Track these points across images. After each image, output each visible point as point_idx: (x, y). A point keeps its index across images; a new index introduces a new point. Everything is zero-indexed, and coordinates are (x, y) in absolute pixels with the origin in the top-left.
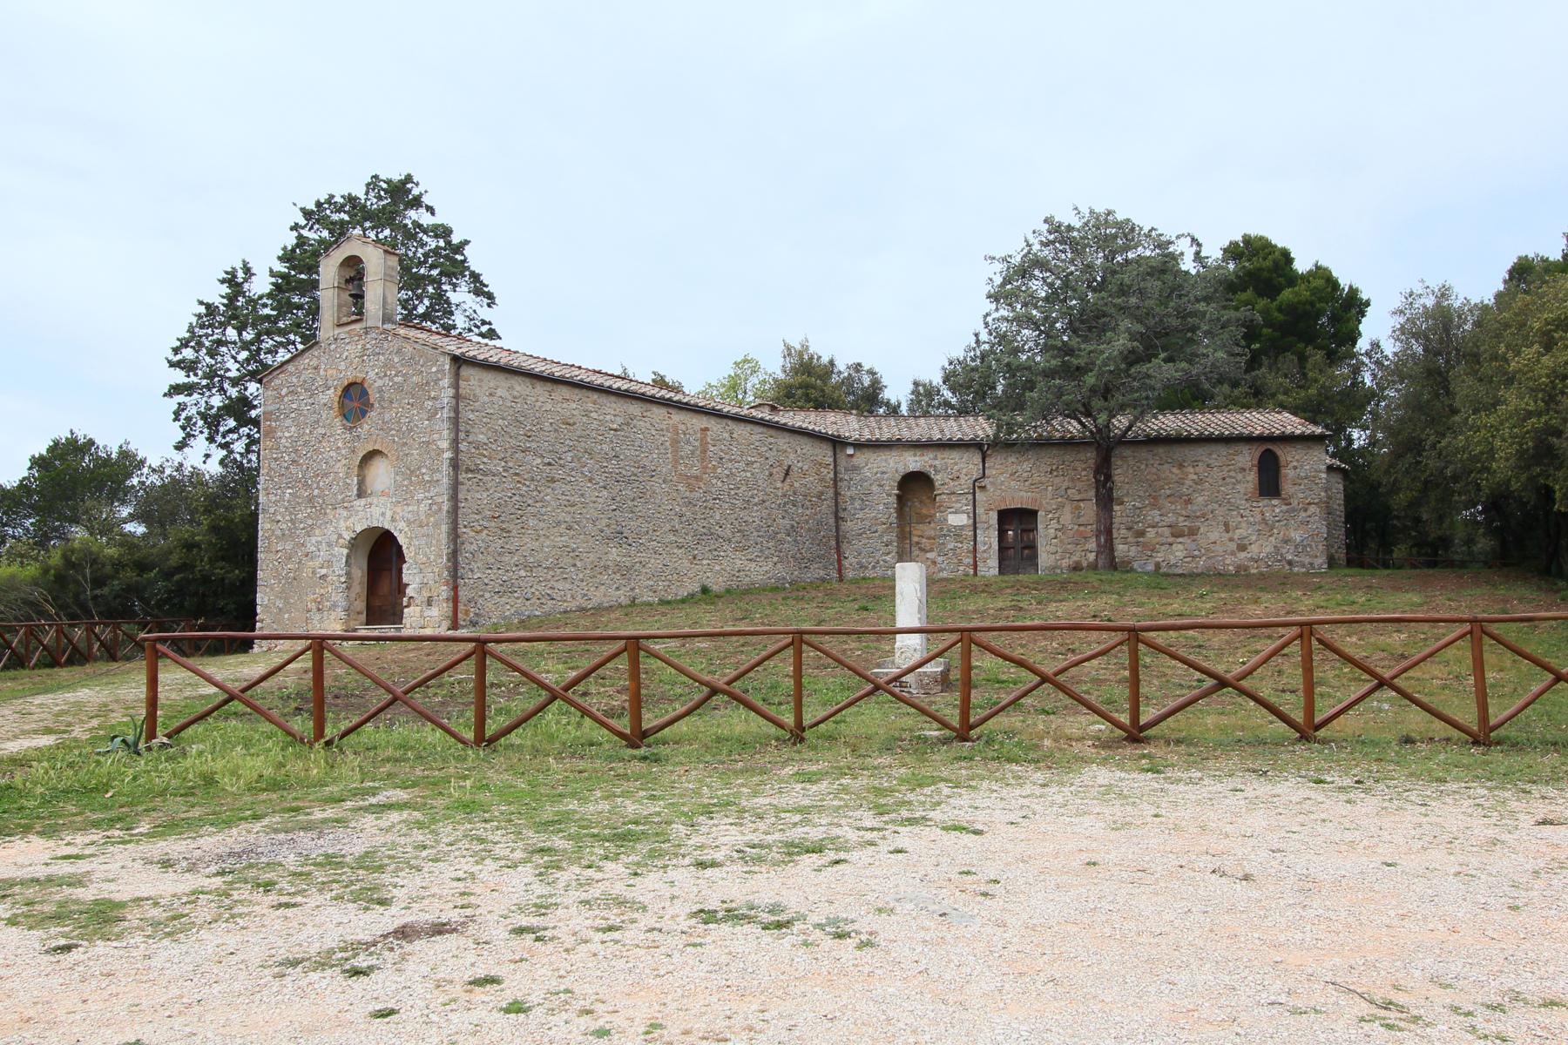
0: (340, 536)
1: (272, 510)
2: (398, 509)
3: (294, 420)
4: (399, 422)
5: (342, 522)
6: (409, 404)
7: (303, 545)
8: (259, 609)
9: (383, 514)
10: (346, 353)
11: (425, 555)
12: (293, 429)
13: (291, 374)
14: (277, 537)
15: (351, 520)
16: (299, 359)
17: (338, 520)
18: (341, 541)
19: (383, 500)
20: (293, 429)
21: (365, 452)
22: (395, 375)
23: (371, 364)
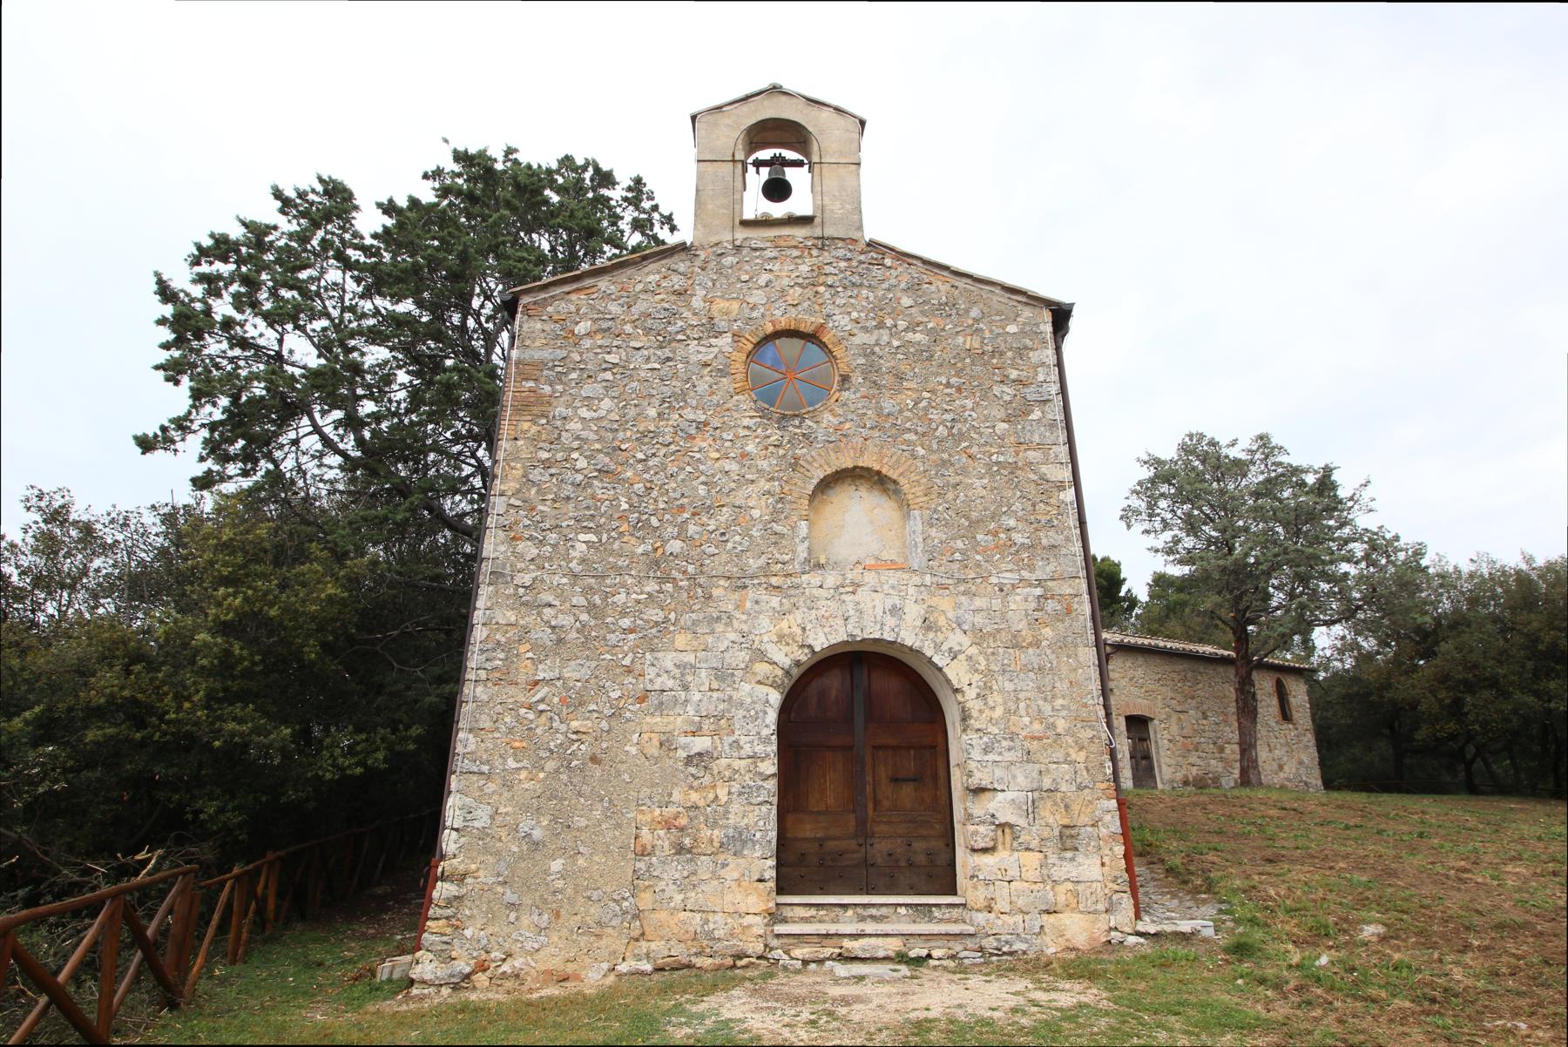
0: (760, 655)
1: (527, 579)
2: (944, 603)
5: (764, 622)
6: (948, 385)
8: (449, 842)
9: (895, 611)
10: (764, 278)
11: (1039, 716)
12: (607, 404)
13: (607, 296)
15: (798, 616)
16: (630, 271)
17: (752, 616)
18: (762, 669)
19: (893, 578)
20: (607, 404)
21: (829, 471)
22: (906, 330)
23: (839, 301)
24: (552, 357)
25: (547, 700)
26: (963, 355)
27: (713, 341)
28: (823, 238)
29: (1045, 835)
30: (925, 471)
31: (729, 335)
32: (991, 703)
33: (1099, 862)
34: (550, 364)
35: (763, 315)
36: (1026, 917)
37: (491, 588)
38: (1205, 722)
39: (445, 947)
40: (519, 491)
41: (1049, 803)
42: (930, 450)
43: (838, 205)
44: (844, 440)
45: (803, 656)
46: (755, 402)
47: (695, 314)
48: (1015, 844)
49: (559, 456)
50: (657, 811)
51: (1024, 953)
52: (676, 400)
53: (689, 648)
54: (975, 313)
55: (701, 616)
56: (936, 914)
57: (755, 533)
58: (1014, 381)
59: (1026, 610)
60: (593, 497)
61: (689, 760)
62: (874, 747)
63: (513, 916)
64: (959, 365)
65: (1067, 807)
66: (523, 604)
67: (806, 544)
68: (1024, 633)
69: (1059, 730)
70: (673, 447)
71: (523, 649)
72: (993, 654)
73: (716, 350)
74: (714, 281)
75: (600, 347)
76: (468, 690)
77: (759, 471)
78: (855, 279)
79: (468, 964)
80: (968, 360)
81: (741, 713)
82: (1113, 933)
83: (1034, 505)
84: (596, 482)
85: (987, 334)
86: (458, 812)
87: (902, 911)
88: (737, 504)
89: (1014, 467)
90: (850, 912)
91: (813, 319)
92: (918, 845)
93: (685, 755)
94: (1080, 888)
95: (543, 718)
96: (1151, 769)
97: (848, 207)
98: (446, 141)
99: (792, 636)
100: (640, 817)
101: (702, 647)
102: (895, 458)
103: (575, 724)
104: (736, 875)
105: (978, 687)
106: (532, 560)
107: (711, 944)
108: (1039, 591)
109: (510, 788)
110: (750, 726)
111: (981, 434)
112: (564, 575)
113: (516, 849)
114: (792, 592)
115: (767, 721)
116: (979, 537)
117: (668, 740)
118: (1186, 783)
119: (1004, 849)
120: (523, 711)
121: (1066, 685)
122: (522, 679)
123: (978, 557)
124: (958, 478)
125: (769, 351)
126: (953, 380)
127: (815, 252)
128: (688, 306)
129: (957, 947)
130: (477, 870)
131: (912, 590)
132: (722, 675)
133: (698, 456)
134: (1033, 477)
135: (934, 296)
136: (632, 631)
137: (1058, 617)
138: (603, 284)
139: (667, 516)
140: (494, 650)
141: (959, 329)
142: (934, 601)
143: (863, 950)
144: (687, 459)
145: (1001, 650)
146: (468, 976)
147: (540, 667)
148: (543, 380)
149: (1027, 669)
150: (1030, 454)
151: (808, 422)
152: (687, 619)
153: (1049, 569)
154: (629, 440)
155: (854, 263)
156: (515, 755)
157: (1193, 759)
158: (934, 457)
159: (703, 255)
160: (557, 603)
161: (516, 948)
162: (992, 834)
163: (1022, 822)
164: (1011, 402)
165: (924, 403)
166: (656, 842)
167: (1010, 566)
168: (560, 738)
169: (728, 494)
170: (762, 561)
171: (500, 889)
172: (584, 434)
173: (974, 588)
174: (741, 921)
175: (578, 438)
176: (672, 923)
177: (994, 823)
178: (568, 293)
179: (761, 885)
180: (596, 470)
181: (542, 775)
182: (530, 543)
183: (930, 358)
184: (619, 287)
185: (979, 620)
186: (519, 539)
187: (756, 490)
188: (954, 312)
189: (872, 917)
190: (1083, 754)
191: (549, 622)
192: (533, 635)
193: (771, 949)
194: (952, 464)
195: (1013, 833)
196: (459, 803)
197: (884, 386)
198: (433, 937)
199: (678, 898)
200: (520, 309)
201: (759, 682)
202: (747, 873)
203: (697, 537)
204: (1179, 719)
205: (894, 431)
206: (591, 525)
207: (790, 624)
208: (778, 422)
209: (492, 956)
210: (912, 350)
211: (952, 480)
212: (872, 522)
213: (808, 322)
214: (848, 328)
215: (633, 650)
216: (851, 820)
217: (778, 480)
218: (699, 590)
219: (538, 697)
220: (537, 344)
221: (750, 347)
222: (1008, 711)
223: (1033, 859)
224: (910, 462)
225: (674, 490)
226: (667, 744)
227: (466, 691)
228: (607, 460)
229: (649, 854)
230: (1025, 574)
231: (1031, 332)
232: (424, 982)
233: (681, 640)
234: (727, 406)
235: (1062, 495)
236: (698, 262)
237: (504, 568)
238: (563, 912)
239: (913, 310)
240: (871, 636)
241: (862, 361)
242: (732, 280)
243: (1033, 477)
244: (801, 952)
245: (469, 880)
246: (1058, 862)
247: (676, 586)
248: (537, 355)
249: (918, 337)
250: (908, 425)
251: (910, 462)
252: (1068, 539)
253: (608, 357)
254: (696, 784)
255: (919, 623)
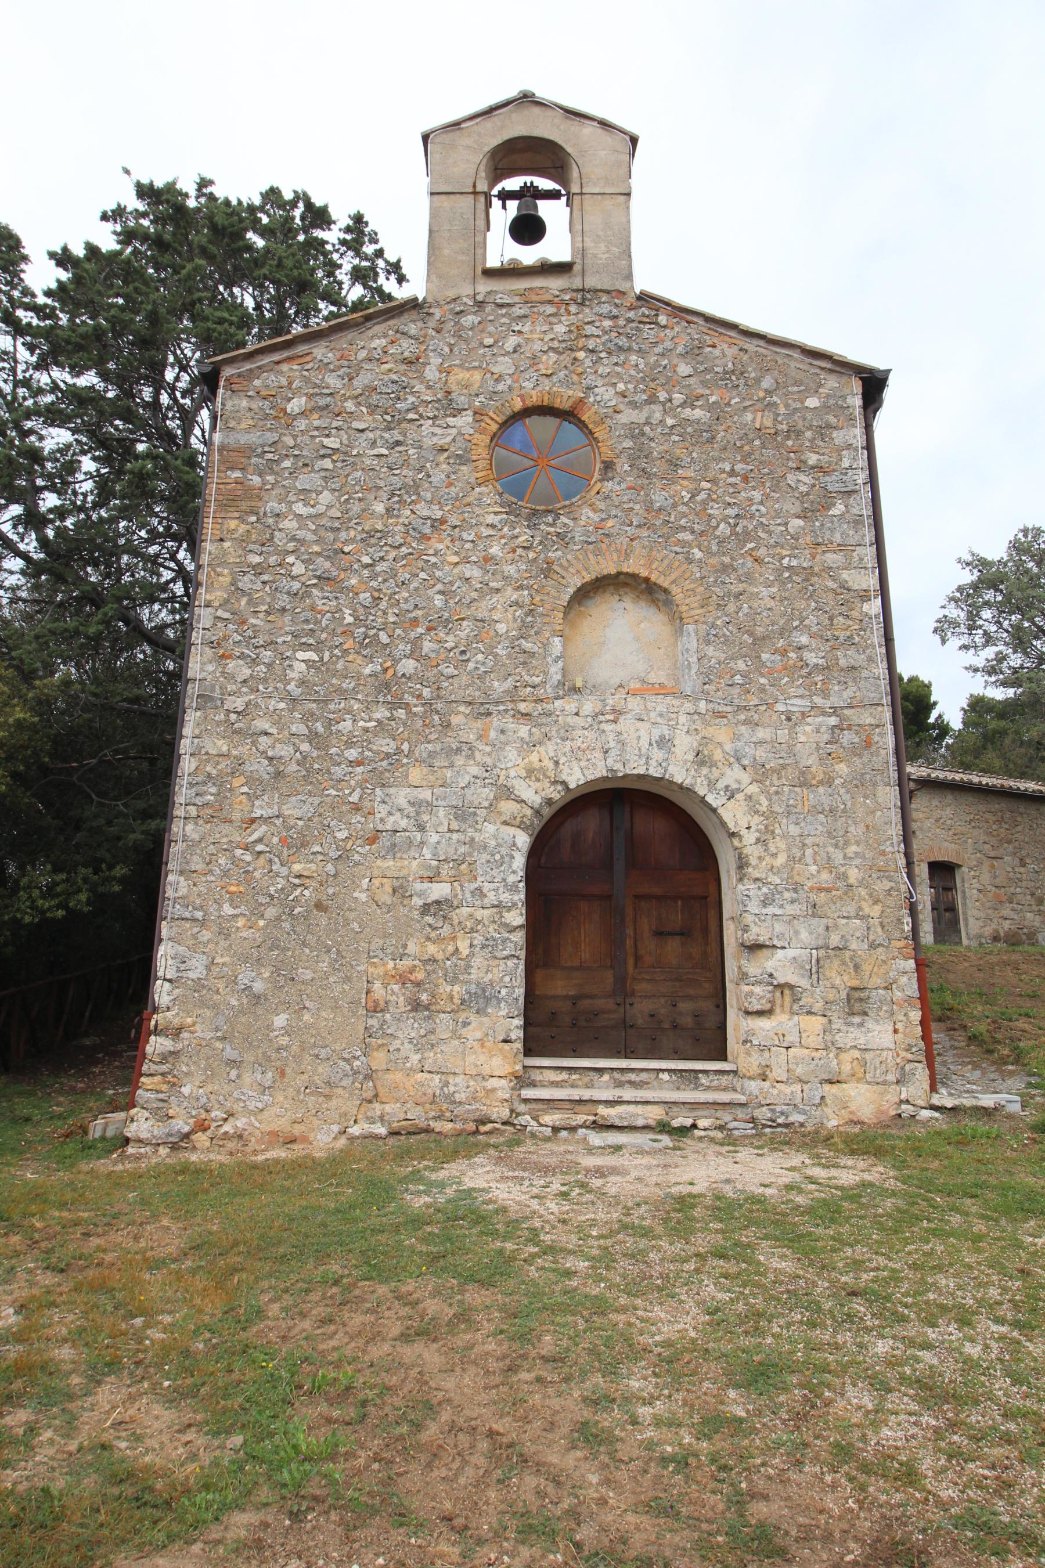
0: (506, 792)
1: (239, 703)
2: (721, 734)
3: (328, 476)
4: (702, 513)
5: (511, 754)
6: (732, 473)
7: (357, 808)
8: (162, 993)
9: (663, 743)
10: (511, 342)
11: (829, 865)
12: (326, 497)
13: (324, 366)
14: (251, 780)
16: (350, 335)
17: (497, 748)
18: (508, 807)
19: (661, 704)
20: (326, 497)
21: (588, 578)
22: (683, 405)
24: (260, 441)
25: (265, 841)
26: (751, 436)
27: (451, 421)
28: (583, 290)
29: (831, 997)
30: (702, 578)
31: (470, 413)
32: (772, 849)
33: (891, 1029)
34: (259, 450)
35: (510, 388)
36: (806, 1087)
37: (199, 713)
38: (1022, 870)
39: (161, 1104)
40: (227, 601)
41: (836, 963)
42: (708, 552)
43: (602, 247)
44: (606, 540)
45: (556, 794)
46: (501, 495)
47: (429, 387)
48: (795, 1007)
49: (272, 560)
50: (391, 964)
51: (802, 1125)
52: (407, 493)
53: (424, 783)
54: (767, 383)
55: (438, 747)
56: (703, 1081)
57: (500, 651)
58: (813, 468)
59: (817, 743)
60: (313, 608)
61: (426, 909)
62: (636, 897)
63: (233, 1074)
64: (746, 448)
65: (856, 967)
66: (235, 732)
67: (560, 664)
68: (813, 769)
69: (852, 880)
70: (404, 550)
71: (236, 782)
72: (777, 793)
73: (454, 431)
74: (451, 347)
75: (317, 429)
76: (176, 827)
77: (505, 578)
78: (623, 341)
79: (186, 1123)
80: (757, 442)
81: (485, 857)
82: (904, 1106)
83: (831, 619)
84: (315, 591)
85: (782, 410)
86: (170, 962)
87: (665, 1076)
88: (480, 616)
89: (809, 572)
90: (606, 1077)
91: (570, 393)
92: (684, 1006)
93: (421, 903)
94: (868, 1056)
95: (262, 860)
96: (954, 924)
97: (615, 250)
98: (127, 172)
99: (543, 770)
100: (371, 970)
101: (440, 782)
102: (666, 562)
103: (297, 867)
104: (478, 1035)
105: (758, 831)
106: (245, 681)
107: (451, 1107)
108: (833, 721)
109: (227, 936)
110: (495, 872)
111: (770, 533)
112: (282, 700)
113: (235, 1003)
114: (544, 720)
115: (515, 866)
116: (765, 656)
117: (402, 886)
118: (996, 939)
119: (783, 1011)
120: (238, 852)
121: (861, 829)
122: (236, 816)
123: (762, 681)
124: (741, 587)
125: (518, 431)
126: (739, 467)
127: (573, 309)
128: (421, 378)
129: (726, 1117)
130: (194, 1024)
131: (683, 719)
132: (463, 814)
133: (433, 559)
134: (831, 584)
135: (717, 362)
136: (359, 763)
137: (854, 751)
138: (320, 351)
139: (398, 632)
140: (204, 783)
141: (748, 403)
142: (710, 731)
143: (621, 1118)
144: (421, 564)
145: (786, 789)
146: (187, 1136)
147: (257, 803)
148: (251, 469)
149: (815, 810)
150: (830, 556)
151: (564, 519)
152: (423, 750)
153: (847, 694)
154: (352, 541)
155: (621, 322)
156: (231, 901)
157: (1006, 912)
158: (713, 561)
159: (438, 313)
160: (273, 731)
161: (238, 1107)
162: (769, 995)
163: (804, 983)
164: (808, 494)
165: (703, 496)
166: (389, 997)
167: (801, 691)
168: (281, 883)
169: (469, 606)
170: (509, 684)
171: (219, 1045)
172: (301, 534)
173: (756, 717)
174: (485, 1084)
175: (293, 539)
176: (408, 1085)
177: (771, 984)
178: (278, 363)
179: (507, 1046)
180: (315, 577)
181: (261, 923)
182: (241, 662)
183: (711, 440)
184: (338, 354)
185: (761, 754)
186: (230, 657)
187: (502, 600)
188: (742, 381)
189: (630, 1082)
190: (877, 909)
191: (264, 752)
192: (248, 767)
193: (518, 1115)
194: (735, 570)
195: (793, 994)
196: (171, 952)
197: (655, 475)
198: (149, 1094)
199: (415, 1058)
200: (222, 383)
201: (505, 823)
202: (491, 1032)
203: (433, 655)
204: (993, 866)
205: (666, 530)
206: (311, 641)
207: (541, 756)
208: (528, 519)
209: (213, 1115)
210: (689, 430)
211: (734, 589)
212: (637, 639)
213: (565, 396)
214: (613, 403)
215: (361, 785)
216: (609, 976)
217: (529, 588)
218: (436, 717)
219: (255, 836)
220: (243, 426)
221: (494, 427)
222: (792, 859)
223: (816, 1023)
224: (685, 566)
225: (406, 600)
226: (400, 891)
227: (175, 829)
228: (327, 564)
229: (382, 1011)
230: (818, 700)
231: (835, 406)
232: (140, 1141)
233: (416, 774)
234: (467, 500)
235: (866, 607)
236: (432, 323)
237: (213, 690)
238: (288, 1071)
239: (692, 380)
240: (635, 772)
241: (628, 444)
242: (473, 345)
243: (831, 584)
244: (550, 1119)
245: (185, 1035)
246: (844, 1028)
247: (409, 712)
248: (244, 439)
249: (698, 413)
250: (683, 522)
251: (685, 566)
252: (871, 660)
253: (326, 441)
254: (433, 935)
255: (691, 756)
